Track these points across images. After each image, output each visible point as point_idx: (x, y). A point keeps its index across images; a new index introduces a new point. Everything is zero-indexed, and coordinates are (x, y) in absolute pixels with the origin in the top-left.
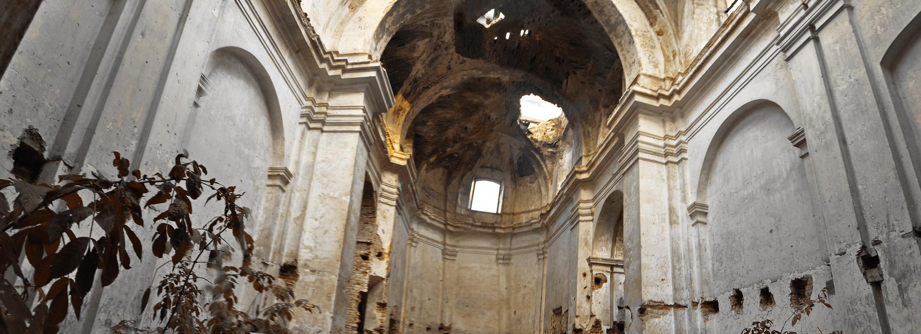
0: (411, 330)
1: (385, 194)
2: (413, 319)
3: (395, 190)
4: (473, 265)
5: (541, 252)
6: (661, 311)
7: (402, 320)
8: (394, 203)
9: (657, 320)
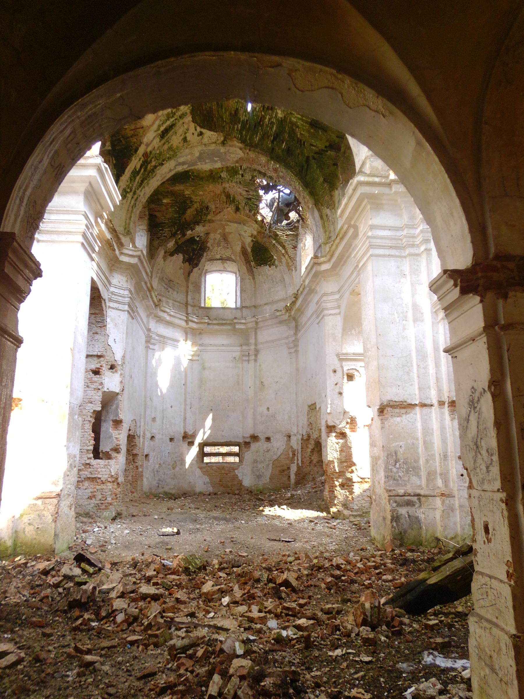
0: (152, 443)
1: (114, 298)
3: (126, 293)
5: (291, 345)
6: (403, 411)
7: (142, 434)
8: (126, 307)
9: (398, 419)
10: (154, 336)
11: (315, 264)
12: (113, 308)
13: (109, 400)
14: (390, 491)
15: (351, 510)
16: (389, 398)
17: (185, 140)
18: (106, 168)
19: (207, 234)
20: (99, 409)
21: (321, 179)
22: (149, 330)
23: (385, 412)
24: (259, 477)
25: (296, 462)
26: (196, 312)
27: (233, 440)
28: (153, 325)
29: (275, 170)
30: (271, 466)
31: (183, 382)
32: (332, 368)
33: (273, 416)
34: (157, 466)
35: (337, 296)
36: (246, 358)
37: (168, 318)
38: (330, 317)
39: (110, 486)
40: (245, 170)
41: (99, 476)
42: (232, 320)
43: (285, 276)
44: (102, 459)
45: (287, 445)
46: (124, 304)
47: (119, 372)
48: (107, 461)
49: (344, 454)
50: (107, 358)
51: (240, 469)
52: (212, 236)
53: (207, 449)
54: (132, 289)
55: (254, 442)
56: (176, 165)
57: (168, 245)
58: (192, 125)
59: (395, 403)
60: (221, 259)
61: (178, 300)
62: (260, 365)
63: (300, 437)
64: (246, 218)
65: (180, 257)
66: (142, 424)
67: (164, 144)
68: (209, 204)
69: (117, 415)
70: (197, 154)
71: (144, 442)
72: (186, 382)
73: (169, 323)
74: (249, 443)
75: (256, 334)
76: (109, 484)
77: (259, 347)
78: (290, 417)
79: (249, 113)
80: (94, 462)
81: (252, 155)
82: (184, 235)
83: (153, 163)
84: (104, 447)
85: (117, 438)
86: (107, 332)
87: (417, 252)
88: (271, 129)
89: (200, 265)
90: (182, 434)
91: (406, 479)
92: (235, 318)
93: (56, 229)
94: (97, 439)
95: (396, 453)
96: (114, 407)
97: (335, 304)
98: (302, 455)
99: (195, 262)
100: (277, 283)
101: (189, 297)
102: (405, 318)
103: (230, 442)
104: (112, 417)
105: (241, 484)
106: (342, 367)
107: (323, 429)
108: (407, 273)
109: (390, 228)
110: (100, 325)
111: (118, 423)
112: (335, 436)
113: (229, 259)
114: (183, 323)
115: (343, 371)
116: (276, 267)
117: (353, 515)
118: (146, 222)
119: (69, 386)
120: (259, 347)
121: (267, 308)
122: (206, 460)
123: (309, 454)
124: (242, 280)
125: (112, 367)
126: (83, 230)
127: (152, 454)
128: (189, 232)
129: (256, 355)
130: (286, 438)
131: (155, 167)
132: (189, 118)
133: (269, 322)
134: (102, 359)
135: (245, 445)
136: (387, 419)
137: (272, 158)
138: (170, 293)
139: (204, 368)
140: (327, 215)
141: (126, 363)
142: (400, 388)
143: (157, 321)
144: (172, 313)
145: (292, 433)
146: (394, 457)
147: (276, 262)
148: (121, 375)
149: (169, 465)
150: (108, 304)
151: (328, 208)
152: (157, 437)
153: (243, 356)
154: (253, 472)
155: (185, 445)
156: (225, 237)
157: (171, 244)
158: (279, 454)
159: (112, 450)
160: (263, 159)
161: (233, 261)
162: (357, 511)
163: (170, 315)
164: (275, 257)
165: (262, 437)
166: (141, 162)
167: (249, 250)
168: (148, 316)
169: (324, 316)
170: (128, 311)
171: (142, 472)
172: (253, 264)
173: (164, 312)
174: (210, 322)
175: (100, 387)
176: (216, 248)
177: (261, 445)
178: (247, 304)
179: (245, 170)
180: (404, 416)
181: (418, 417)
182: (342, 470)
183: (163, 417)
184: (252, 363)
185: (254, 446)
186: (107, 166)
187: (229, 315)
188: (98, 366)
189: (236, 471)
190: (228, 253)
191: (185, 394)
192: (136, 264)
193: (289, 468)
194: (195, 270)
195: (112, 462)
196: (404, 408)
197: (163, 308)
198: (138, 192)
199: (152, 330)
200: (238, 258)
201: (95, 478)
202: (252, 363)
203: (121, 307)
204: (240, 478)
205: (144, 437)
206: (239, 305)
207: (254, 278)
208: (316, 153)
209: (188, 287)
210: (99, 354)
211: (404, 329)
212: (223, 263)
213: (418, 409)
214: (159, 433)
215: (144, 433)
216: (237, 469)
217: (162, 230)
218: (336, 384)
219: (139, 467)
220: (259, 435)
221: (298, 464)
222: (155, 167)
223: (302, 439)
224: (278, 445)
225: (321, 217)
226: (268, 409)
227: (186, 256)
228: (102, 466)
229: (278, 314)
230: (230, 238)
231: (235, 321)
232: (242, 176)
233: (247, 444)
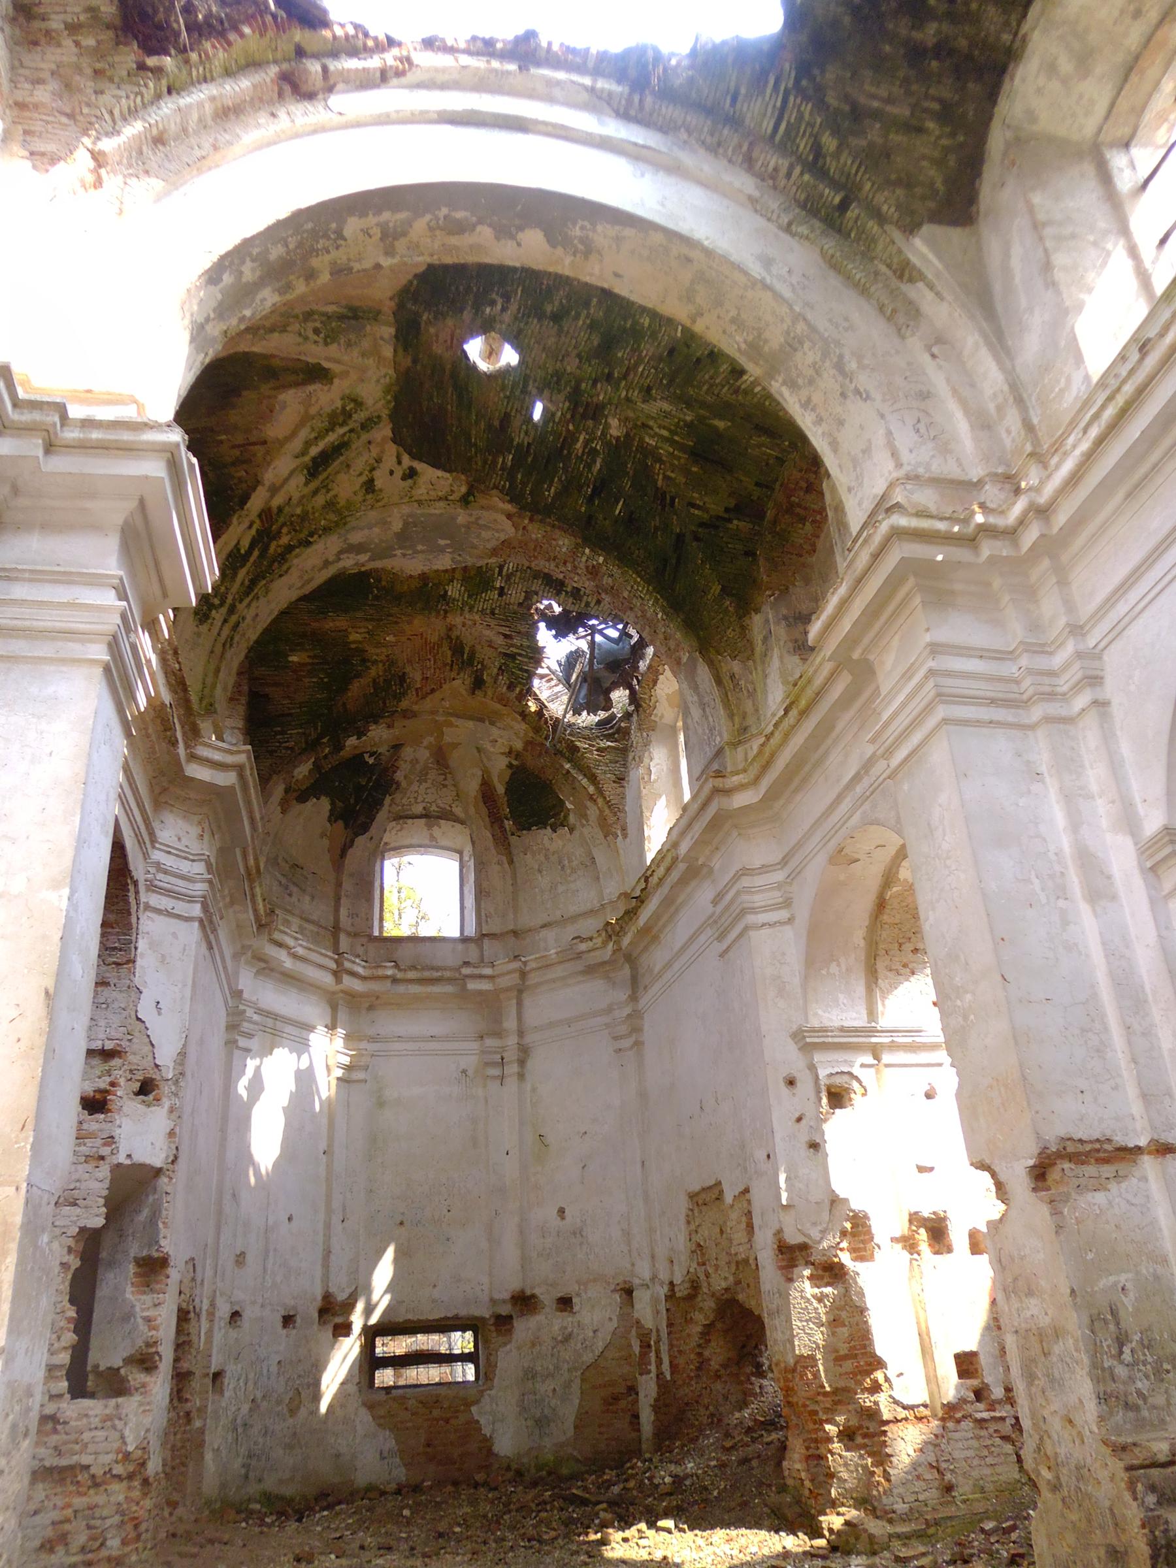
0: (233, 1334)
1: (164, 880)
2: (239, 1295)
3: (199, 868)
5: (623, 1029)
6: (1107, 1170)
7: (205, 1307)
8: (196, 910)
10: (250, 1012)
11: (716, 791)
12: (158, 911)
13: (132, 1191)
14: (1124, 1448)
15: (888, 1516)
16: (1062, 1133)
17: (369, 486)
18: (191, 465)
19: (397, 747)
20: (97, 1221)
21: (716, 589)
22: (238, 994)
23: (1054, 1175)
24: (541, 1423)
25: (653, 1368)
26: (360, 950)
27: (463, 1312)
28: (247, 981)
29: (593, 572)
30: (576, 1387)
31: (323, 1146)
32: (784, 1072)
33: (578, 1233)
34: (245, 1408)
35: (779, 876)
36: (495, 1072)
37: (288, 963)
38: (765, 932)
39: (118, 1492)
40: (509, 577)
41: (85, 1460)
42: (458, 969)
43: (596, 853)
44: (92, 1395)
45: (621, 1317)
46: (190, 899)
47: (166, 1103)
48: (112, 1402)
49: (844, 1332)
50: (131, 1058)
51: (486, 1400)
52: (407, 752)
53: (387, 1347)
54: (213, 860)
56: (341, 552)
57: (296, 772)
58: (392, 449)
59: (1080, 1148)
60: (426, 815)
61: (315, 918)
62: (534, 1090)
63: (663, 1291)
64: (499, 706)
65: (325, 804)
66: (209, 1273)
67: (315, 492)
68: (408, 669)
69: (154, 1241)
70: (397, 526)
71: (210, 1332)
72: (330, 1145)
73: (290, 979)
74: (510, 1317)
75: (520, 1004)
76: (116, 1487)
77: (528, 1039)
78: (627, 1234)
79: (535, 425)
80: (71, 1409)
81: (537, 532)
82: (338, 747)
83: (285, 540)
84: (108, 1353)
85: (148, 1320)
86: (137, 980)
87: (1064, 712)
88: (588, 467)
89: (373, 830)
90: (318, 1303)
91: (1160, 1400)
92: (467, 964)
93: (27, 623)
94: (83, 1326)
95: (1114, 1312)
96: (145, 1213)
97: (776, 896)
98: (671, 1346)
99: (362, 819)
100: (574, 871)
101: (343, 912)
102: (1062, 892)
103: (456, 1317)
104: (135, 1249)
105: (490, 1451)
106: (812, 1068)
107: (766, 1257)
108: (1043, 769)
109: (982, 654)
110: (118, 957)
111: (153, 1267)
112: (810, 1278)
113: (446, 815)
114: (327, 979)
115: (817, 1078)
116: (571, 830)
117: (898, 1536)
118: (241, 709)
119: (30, 1126)
120: (528, 1039)
121: (550, 935)
122: (385, 1377)
123: (695, 1340)
124: (481, 867)
125: (146, 1088)
126: (111, 628)
127: (232, 1370)
128: (352, 741)
129: (522, 1062)
130: (617, 1297)
131: (290, 548)
132: (384, 431)
133: (559, 972)
134: (116, 1062)
135: (491, 1327)
136: (1066, 1198)
137: (587, 541)
138: (294, 899)
139: (381, 1104)
140: (732, 677)
141: (188, 1074)
143: (259, 973)
144: (300, 951)
145: (636, 1281)
146: (1112, 1327)
147: (572, 819)
148: (172, 1110)
149: (279, 1402)
150: (143, 898)
151: (734, 658)
152: (247, 1314)
153: (487, 1064)
154: (523, 1409)
156: (441, 757)
157: (303, 770)
158: (600, 1345)
159: (129, 1361)
160: (564, 543)
161: (457, 820)
162: (905, 1518)
163: (295, 956)
164: (569, 806)
165: (547, 1297)
166: (253, 532)
167: (501, 789)
168: (236, 956)
169: (746, 928)
170: (201, 921)
171: (202, 1431)
172: (508, 824)
173: (280, 945)
174: (400, 975)
175: (105, 1151)
176: (415, 787)
177: (544, 1324)
178: (494, 927)
179: (509, 577)
180: (1113, 1186)
181: (1155, 1187)
182: (841, 1384)
183: (267, 1252)
184: (512, 1083)
185: (524, 1328)
186: (195, 460)
187: (449, 958)
188: (103, 1084)
189: (474, 1409)
190: (444, 799)
191: (328, 1180)
192: (231, 788)
193: (632, 1390)
194: (360, 841)
195: (130, 1405)
196: (1106, 1161)
197: (277, 936)
198: (240, 607)
199: (245, 995)
200: (472, 811)
201: (71, 1468)
202: (512, 1083)
203: (181, 907)
204: (487, 1431)
205: (211, 1315)
206: (471, 931)
207: (511, 862)
208: (702, 525)
209: (339, 885)
210: (109, 1045)
211: (1065, 923)
212: (429, 827)
213: (1148, 1163)
214: (254, 1303)
215: (213, 1304)
216: (477, 1402)
217: (283, 733)
218: (799, 1120)
219: (194, 1414)
220: (537, 1291)
221: (660, 1375)
222: (290, 548)
223: (668, 1298)
224: (597, 1317)
225: (719, 681)
226: (561, 1211)
227: (340, 804)
228: (95, 1422)
229: (583, 947)
230: (454, 758)
231: (466, 971)
232: (502, 592)
233: (503, 1323)
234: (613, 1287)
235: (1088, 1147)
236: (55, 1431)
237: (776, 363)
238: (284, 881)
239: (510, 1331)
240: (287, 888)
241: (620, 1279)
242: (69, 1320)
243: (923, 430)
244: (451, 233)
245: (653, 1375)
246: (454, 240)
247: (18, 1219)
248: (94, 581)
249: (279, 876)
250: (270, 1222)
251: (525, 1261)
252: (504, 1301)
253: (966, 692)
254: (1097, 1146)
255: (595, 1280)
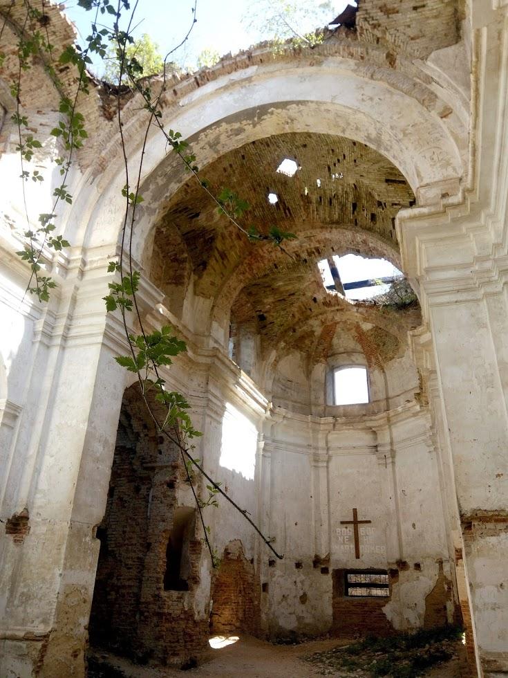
4: (349, 471)
5: (430, 442)
36: (383, 461)
41: (171, 611)
48: (182, 592)
53: (353, 578)
55: (402, 569)
68: (315, 296)
75: (391, 430)
76: (181, 622)
77: (395, 447)
78: (439, 536)
90: (313, 558)
109: (454, 267)
121: (402, 399)
122: (352, 591)
129: (393, 457)
133: (404, 416)
136: (474, 539)
142: (492, 489)
144: (289, 415)
145: (444, 559)
155: (318, 572)
165: (411, 564)
183: (286, 538)
184: (390, 466)
193: (445, 608)
205: (259, 561)
220: (407, 560)
226: (414, 525)
234: (436, 560)
235: (490, 514)
236: (158, 600)
237: (378, 141)
238: (283, 388)
239: (398, 576)
240: (285, 390)
241: (439, 557)
242: (164, 562)
243: (435, 157)
244: (237, 135)
245: (452, 601)
246: (239, 137)
247: (67, 533)
248: (99, 314)
249: (281, 386)
250: (287, 525)
251: (400, 546)
252: (393, 564)
253: (436, 290)
254: (497, 513)
255: (429, 557)
